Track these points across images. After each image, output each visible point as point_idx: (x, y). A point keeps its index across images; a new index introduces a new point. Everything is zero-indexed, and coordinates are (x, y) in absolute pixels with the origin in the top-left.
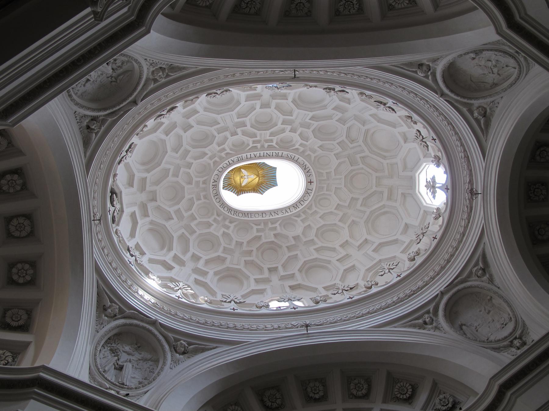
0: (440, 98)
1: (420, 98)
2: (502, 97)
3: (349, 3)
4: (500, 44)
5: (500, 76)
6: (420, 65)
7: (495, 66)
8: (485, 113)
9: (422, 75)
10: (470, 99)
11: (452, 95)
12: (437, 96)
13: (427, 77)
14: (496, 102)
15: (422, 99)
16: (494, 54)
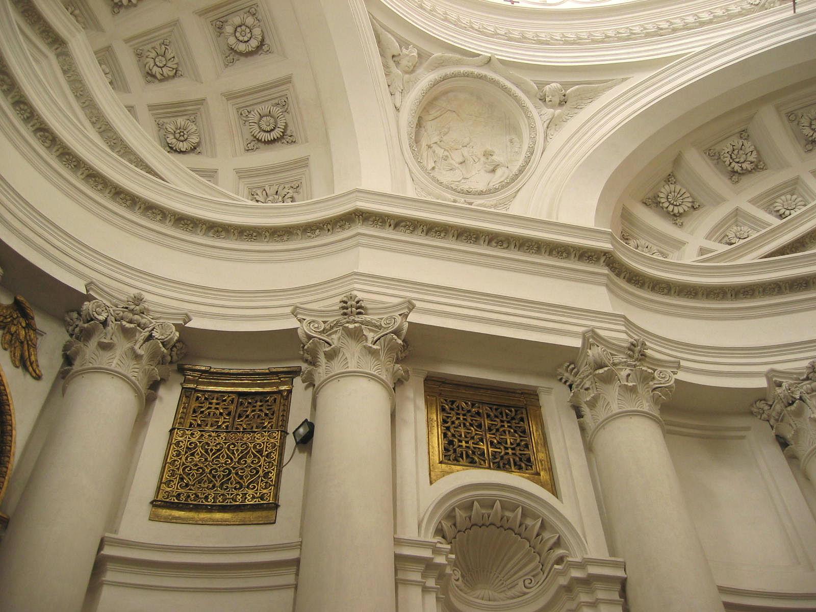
0: (490, 55)
1: (499, 34)
2: (397, 109)
3: (742, 160)
4: (501, 204)
5: (427, 145)
6: (563, 102)
7: (446, 158)
8: (397, 64)
9: (553, 85)
10: (445, 78)
11: (476, 71)
12: (497, 57)
13: (541, 85)
14: (398, 95)
15: (495, 34)
16: (468, 179)
